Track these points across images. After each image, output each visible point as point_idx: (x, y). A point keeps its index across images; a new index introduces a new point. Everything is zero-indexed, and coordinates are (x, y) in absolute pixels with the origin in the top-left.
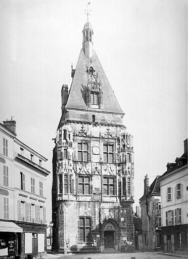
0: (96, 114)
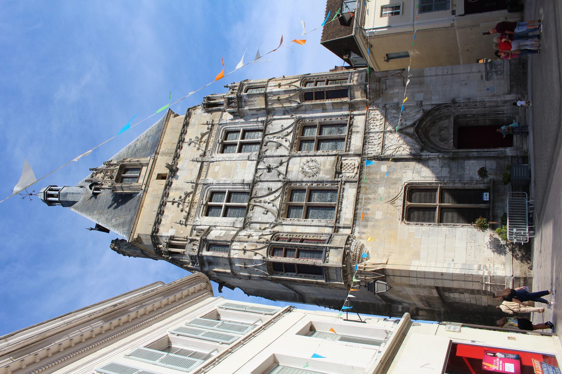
0: (156, 171)
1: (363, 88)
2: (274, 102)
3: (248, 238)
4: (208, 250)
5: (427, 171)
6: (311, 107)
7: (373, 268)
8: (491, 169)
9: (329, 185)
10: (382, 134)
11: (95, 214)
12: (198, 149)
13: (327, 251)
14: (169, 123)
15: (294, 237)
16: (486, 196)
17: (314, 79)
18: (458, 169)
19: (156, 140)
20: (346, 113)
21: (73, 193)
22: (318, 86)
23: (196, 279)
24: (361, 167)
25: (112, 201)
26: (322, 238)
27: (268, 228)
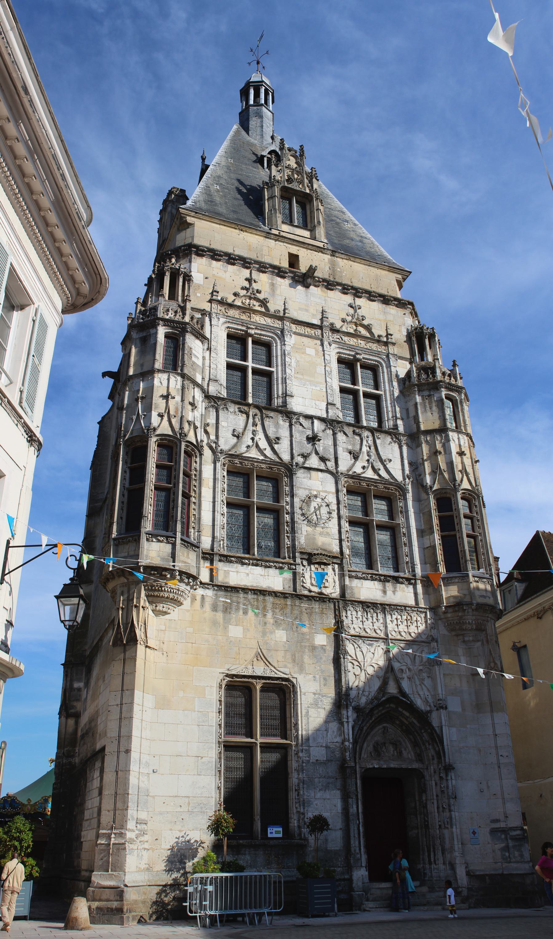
1: (466, 600)
2: (432, 445)
3: (190, 403)
4: (167, 336)
5: (319, 719)
6: (426, 510)
7: (138, 622)
8: (326, 840)
9: (288, 542)
10: (382, 635)
11: (228, 160)
12: (343, 321)
13: (167, 540)
14: (387, 272)
15: (194, 482)
16: (277, 832)
17: (477, 513)
18: (324, 777)
19: (357, 252)
20: (418, 570)
21: (262, 126)
22: (464, 521)
23: (95, 274)
24: (322, 598)
25: (250, 186)
26: (191, 530)
27: (208, 437)
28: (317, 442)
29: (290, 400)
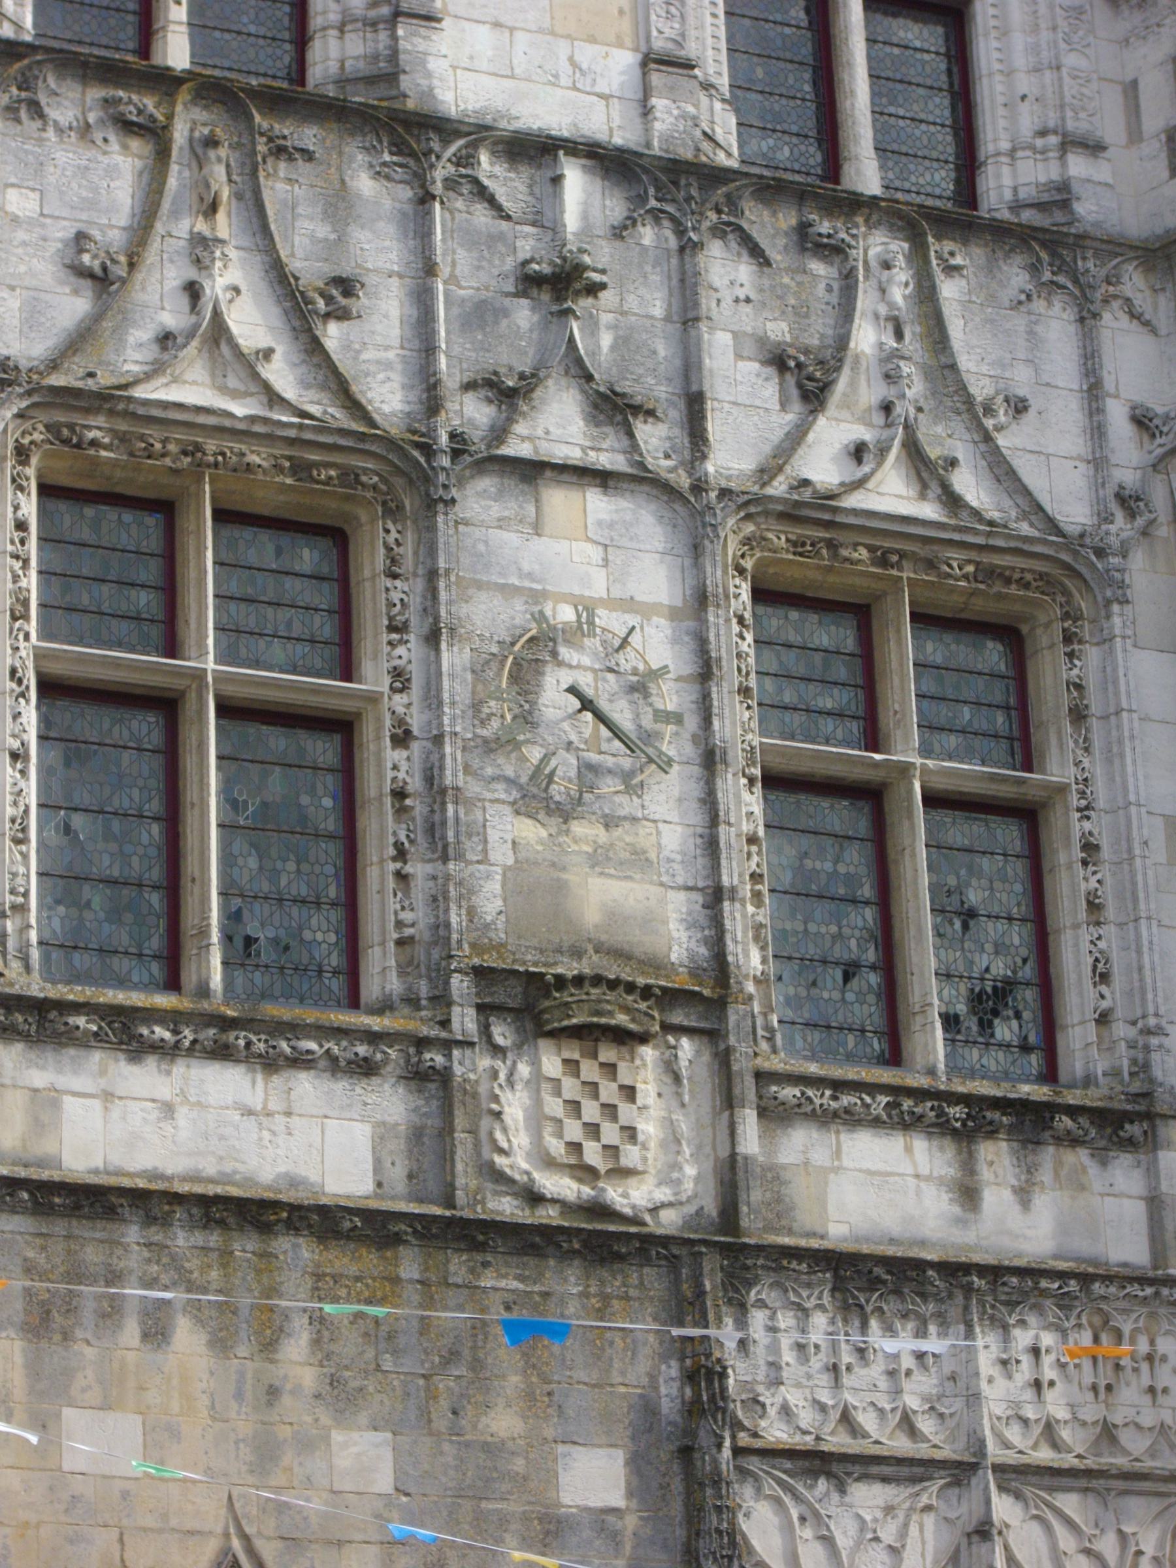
28: (586, 302)
29: (421, 45)
